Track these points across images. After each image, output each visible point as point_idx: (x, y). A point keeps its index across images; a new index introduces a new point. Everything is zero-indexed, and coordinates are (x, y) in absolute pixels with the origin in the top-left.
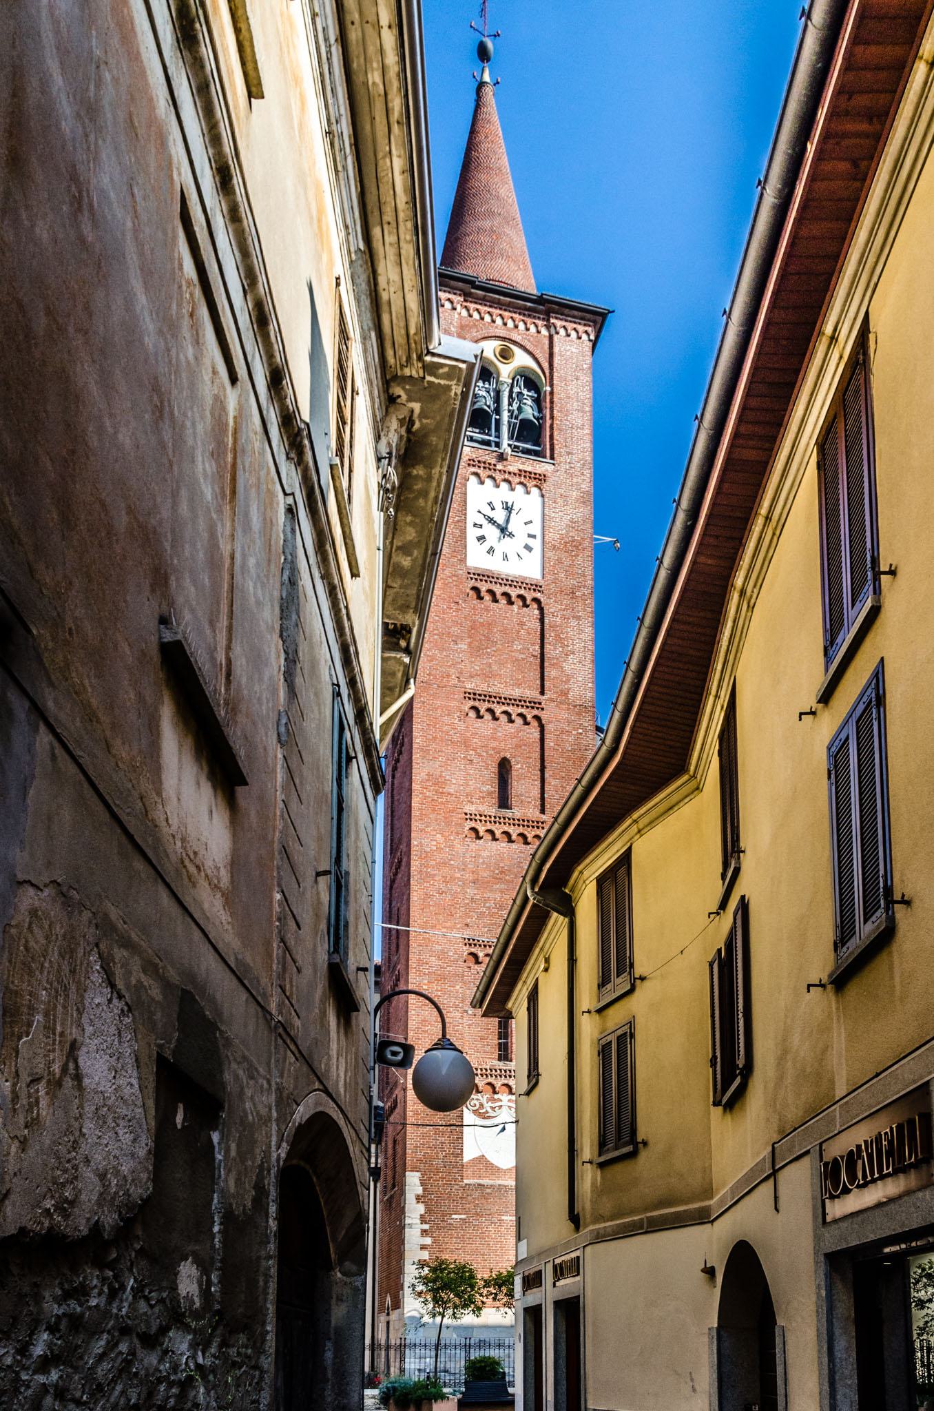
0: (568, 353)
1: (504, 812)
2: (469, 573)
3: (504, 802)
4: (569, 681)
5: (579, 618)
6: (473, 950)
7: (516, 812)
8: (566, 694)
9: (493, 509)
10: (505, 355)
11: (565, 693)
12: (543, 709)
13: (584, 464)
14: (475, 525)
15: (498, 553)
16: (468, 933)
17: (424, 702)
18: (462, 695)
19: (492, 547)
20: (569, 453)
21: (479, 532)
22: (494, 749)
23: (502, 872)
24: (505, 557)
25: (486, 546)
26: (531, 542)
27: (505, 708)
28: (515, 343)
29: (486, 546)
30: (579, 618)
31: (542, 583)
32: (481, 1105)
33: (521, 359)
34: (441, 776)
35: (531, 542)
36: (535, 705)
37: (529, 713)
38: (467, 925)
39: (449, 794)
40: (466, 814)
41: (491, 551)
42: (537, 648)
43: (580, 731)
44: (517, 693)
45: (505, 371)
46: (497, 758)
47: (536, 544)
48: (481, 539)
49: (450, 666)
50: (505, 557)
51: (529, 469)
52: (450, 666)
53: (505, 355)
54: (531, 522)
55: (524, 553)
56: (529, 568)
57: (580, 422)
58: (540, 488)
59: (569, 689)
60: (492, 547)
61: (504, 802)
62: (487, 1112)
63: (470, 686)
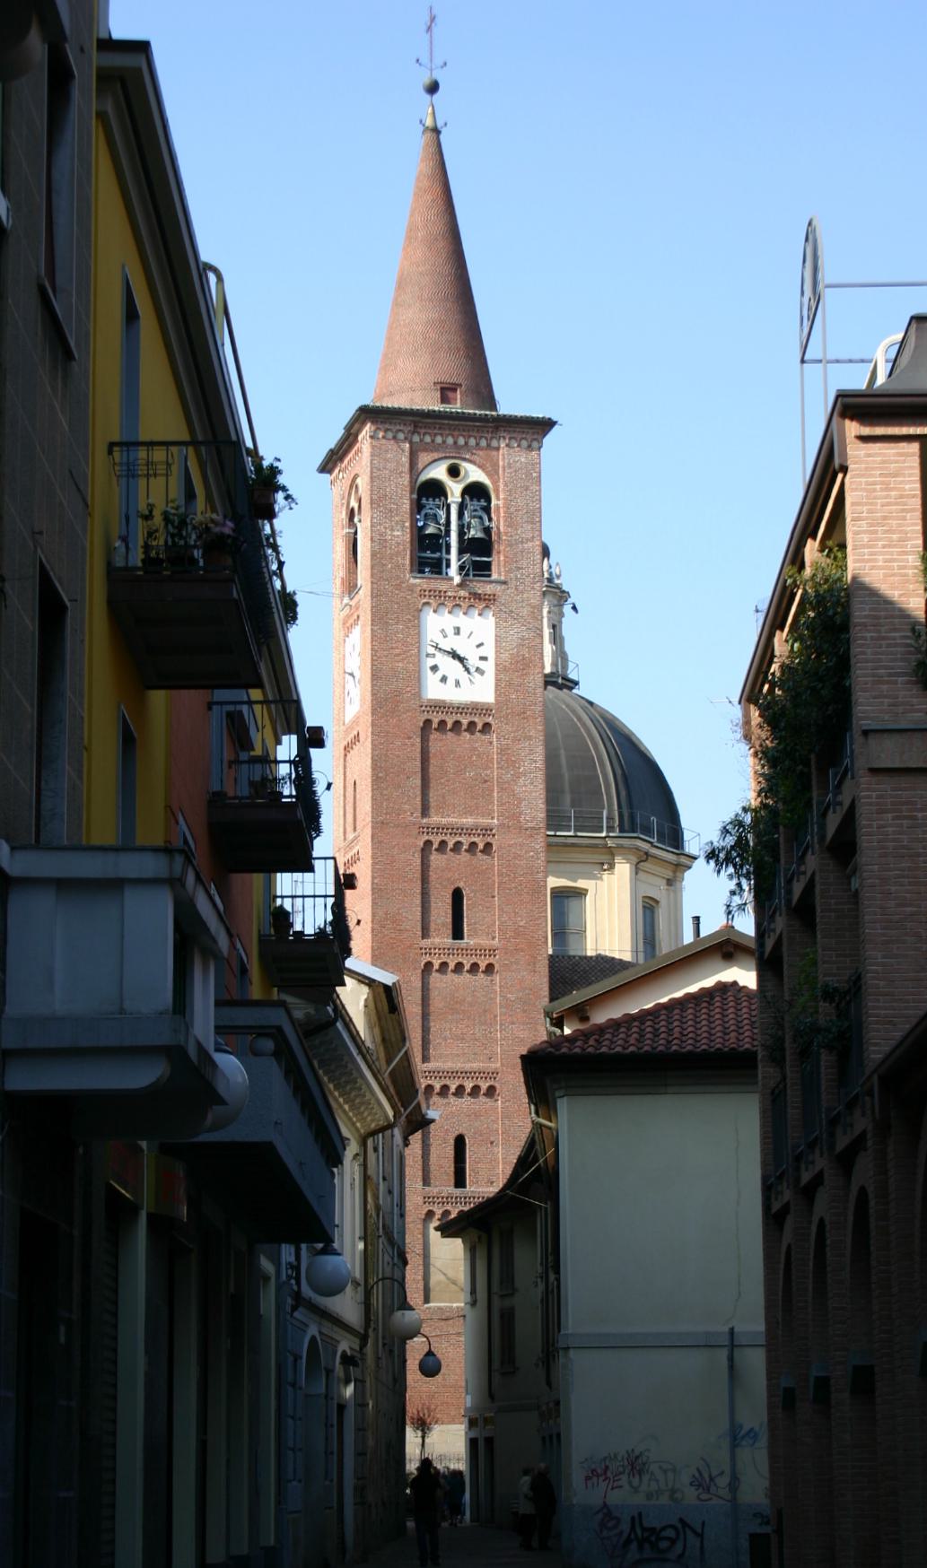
0: (518, 464)
4: (520, 803)
5: (530, 738)
7: (468, 941)
9: (445, 636)
10: (454, 472)
11: (516, 817)
13: (534, 578)
15: (451, 682)
20: (519, 569)
22: (449, 879)
24: (457, 683)
25: (439, 675)
26: (482, 665)
29: (439, 675)
30: (530, 738)
31: (493, 707)
33: (474, 473)
34: (399, 913)
35: (482, 665)
36: (487, 830)
40: (421, 949)
41: (444, 679)
43: (532, 854)
45: (455, 490)
46: (453, 887)
50: (457, 683)
56: (481, 690)
59: (520, 814)
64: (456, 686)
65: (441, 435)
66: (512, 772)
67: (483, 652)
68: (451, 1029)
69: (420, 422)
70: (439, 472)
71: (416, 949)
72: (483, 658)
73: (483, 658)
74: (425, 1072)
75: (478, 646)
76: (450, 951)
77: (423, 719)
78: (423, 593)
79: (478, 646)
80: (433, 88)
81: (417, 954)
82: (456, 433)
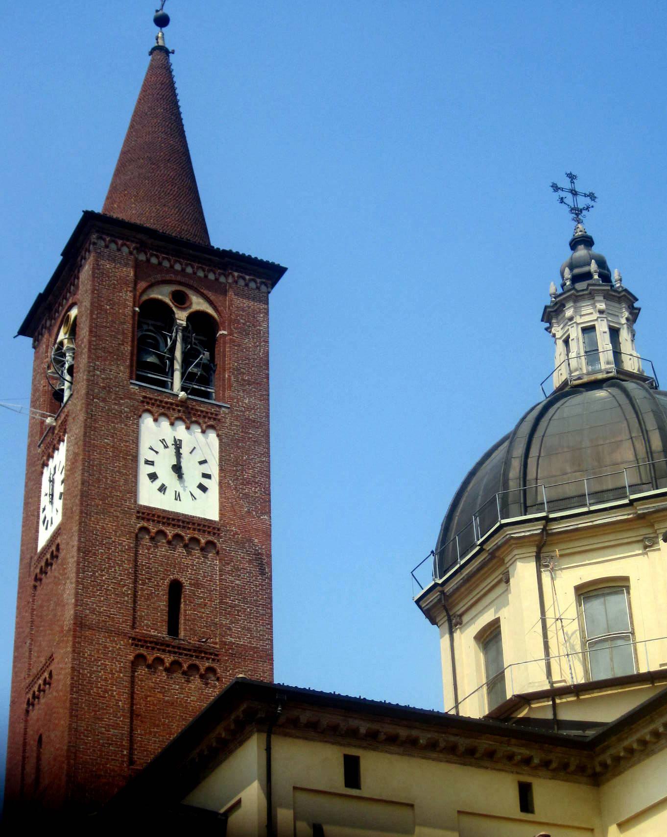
14: (147, 462)
19: (163, 485)
21: (150, 469)
24: (178, 497)
25: (158, 483)
26: (205, 482)
28: (191, 287)
29: (158, 483)
33: (198, 304)
35: (205, 482)
41: (162, 489)
45: (181, 317)
47: (213, 485)
48: (153, 477)
50: (178, 497)
53: (181, 299)
54: (204, 462)
55: (198, 492)
60: (163, 485)
64: (176, 499)
67: (205, 469)
70: (163, 294)
72: (207, 476)
73: (207, 476)
75: (201, 463)
78: (146, 400)
79: (201, 463)
80: (162, 21)
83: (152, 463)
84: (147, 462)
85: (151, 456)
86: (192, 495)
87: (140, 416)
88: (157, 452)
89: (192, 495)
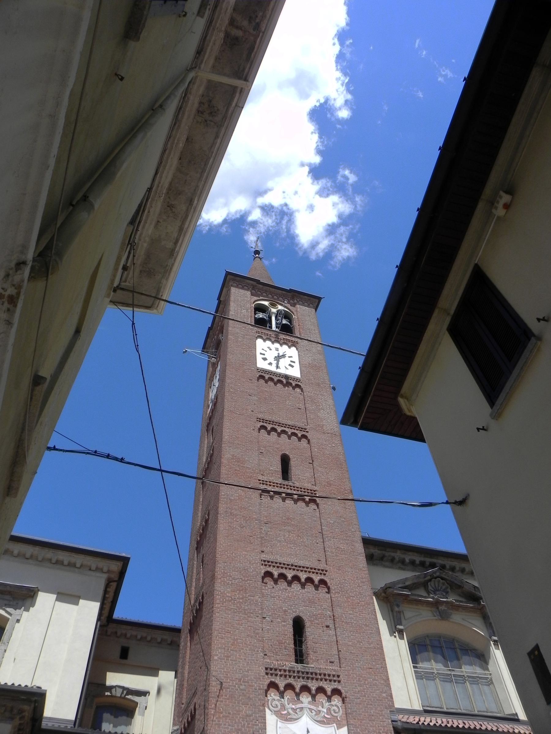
1: (286, 483)
2: (258, 370)
3: (300, 657)
6: (269, 569)
8: (322, 427)
12: (307, 432)
16: (264, 556)
17: (230, 420)
18: (256, 420)
22: (277, 448)
23: (288, 519)
25: (268, 362)
26: (292, 364)
27: (283, 428)
32: (283, 706)
35: (292, 364)
37: (300, 433)
38: (263, 552)
39: (248, 468)
40: (259, 480)
42: (302, 406)
44: (290, 423)
46: (281, 453)
48: (265, 359)
49: (247, 405)
51: (289, 339)
52: (247, 405)
57: (313, 328)
58: (295, 346)
61: (300, 657)
62: (289, 714)
63: (260, 416)
65: (266, 293)
66: (315, 407)
68: (284, 536)
69: (256, 286)
71: (255, 479)
74: (265, 561)
76: (281, 486)
77: (259, 374)
81: (256, 482)
82: (273, 294)
83: (264, 354)
84: (261, 354)
85: (263, 352)
86: (286, 368)
87: (257, 338)
88: (266, 351)
89: (286, 368)
